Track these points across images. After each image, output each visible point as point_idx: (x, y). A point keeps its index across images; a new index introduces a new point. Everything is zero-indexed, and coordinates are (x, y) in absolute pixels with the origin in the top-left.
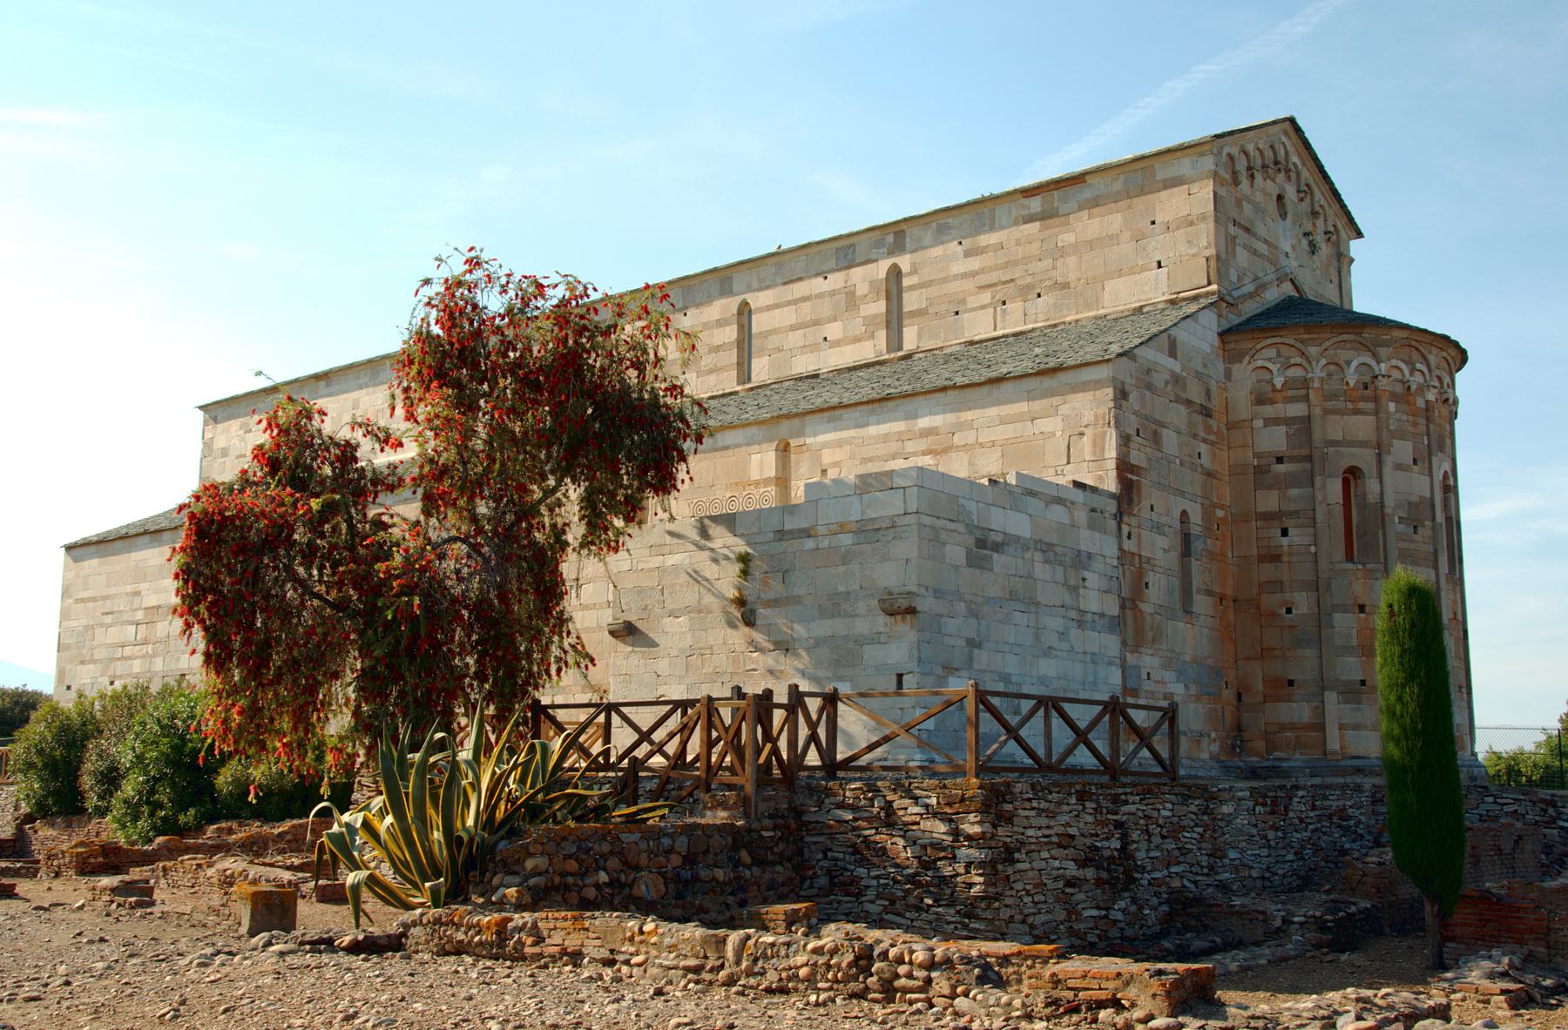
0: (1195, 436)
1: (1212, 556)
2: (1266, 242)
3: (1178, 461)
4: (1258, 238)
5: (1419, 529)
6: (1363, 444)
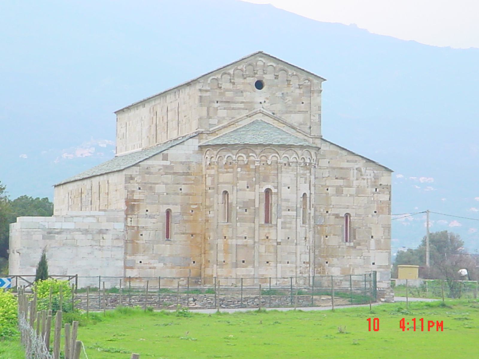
0: (178, 184)
1: (186, 221)
2: (242, 102)
3: (165, 194)
4: (238, 103)
5: (247, 210)
6: (227, 183)
